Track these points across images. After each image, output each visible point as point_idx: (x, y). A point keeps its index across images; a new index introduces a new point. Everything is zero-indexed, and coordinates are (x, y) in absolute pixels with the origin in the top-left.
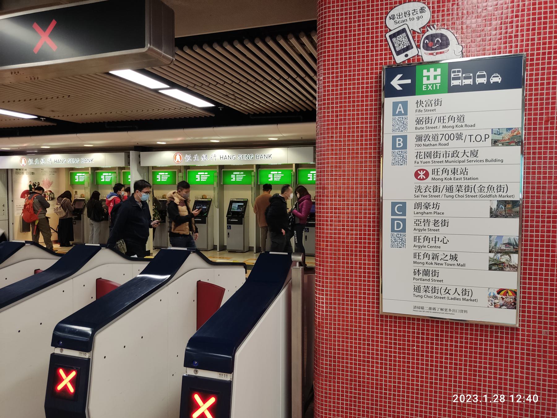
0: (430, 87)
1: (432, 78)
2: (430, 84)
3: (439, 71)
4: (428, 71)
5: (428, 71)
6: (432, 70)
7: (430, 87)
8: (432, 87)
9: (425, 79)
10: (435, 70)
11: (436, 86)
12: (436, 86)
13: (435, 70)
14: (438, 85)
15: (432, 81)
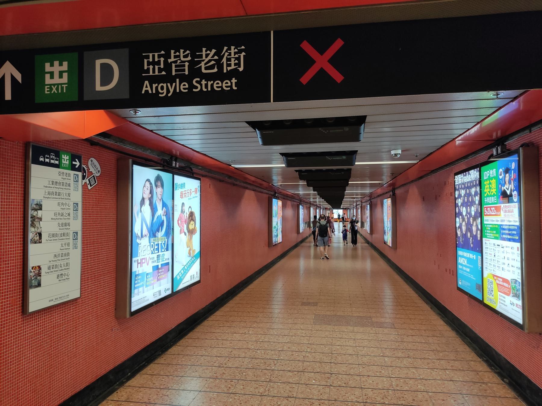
0: (54, 89)
1: (56, 75)
2: (54, 85)
3: (65, 64)
4: (52, 65)
5: (52, 65)
6: (56, 63)
7: (54, 89)
8: (57, 89)
9: (47, 76)
10: (61, 64)
11: (62, 88)
12: (62, 88)
13: (61, 64)
14: (65, 86)
15: (57, 80)
